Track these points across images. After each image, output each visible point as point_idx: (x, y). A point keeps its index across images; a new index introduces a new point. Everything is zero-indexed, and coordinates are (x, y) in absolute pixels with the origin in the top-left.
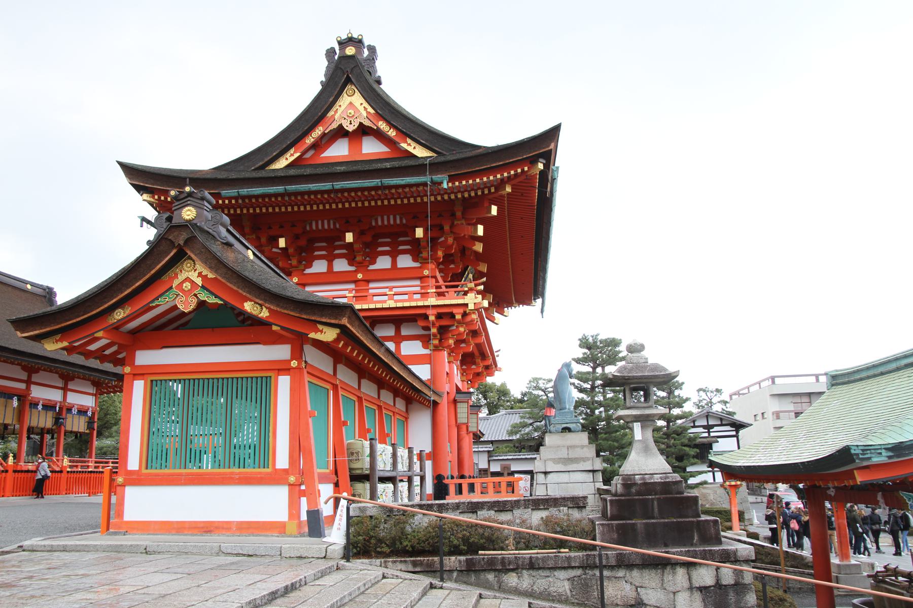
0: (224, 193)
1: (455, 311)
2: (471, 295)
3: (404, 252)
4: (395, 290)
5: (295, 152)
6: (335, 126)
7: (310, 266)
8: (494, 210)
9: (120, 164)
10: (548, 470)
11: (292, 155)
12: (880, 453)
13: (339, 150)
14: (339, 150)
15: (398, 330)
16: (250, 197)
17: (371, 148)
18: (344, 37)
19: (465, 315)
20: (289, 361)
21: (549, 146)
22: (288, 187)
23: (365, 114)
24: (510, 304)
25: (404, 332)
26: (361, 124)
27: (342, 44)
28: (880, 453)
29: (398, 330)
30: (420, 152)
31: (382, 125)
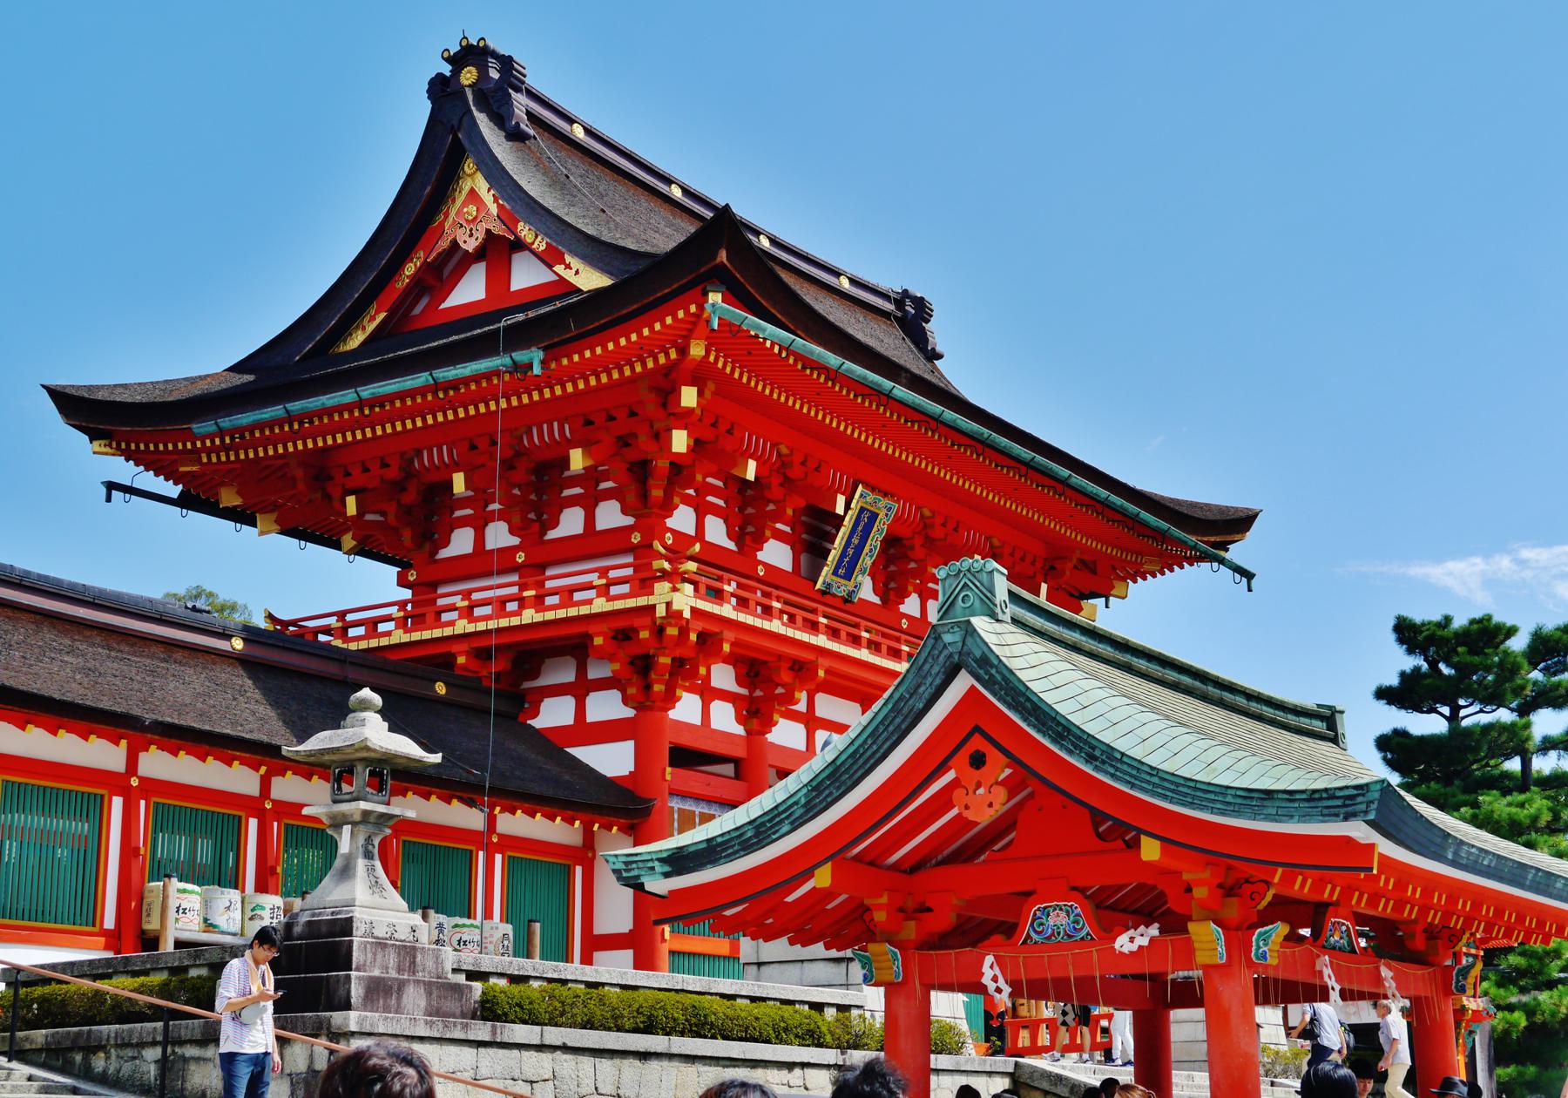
0: (199, 428)
1: (637, 622)
2: (662, 588)
3: (608, 495)
4: (475, 596)
5: (377, 312)
6: (444, 244)
7: (446, 543)
8: (689, 397)
10: (764, 959)
11: (373, 319)
12: (653, 868)
13: (471, 290)
14: (471, 290)
15: (581, 671)
16: (241, 430)
17: (526, 275)
22: (290, 406)
23: (494, 209)
24: (1138, 573)
25: (594, 673)
26: (488, 231)
27: (458, 60)
28: (653, 868)
29: (581, 671)
30: (589, 279)
31: (525, 231)
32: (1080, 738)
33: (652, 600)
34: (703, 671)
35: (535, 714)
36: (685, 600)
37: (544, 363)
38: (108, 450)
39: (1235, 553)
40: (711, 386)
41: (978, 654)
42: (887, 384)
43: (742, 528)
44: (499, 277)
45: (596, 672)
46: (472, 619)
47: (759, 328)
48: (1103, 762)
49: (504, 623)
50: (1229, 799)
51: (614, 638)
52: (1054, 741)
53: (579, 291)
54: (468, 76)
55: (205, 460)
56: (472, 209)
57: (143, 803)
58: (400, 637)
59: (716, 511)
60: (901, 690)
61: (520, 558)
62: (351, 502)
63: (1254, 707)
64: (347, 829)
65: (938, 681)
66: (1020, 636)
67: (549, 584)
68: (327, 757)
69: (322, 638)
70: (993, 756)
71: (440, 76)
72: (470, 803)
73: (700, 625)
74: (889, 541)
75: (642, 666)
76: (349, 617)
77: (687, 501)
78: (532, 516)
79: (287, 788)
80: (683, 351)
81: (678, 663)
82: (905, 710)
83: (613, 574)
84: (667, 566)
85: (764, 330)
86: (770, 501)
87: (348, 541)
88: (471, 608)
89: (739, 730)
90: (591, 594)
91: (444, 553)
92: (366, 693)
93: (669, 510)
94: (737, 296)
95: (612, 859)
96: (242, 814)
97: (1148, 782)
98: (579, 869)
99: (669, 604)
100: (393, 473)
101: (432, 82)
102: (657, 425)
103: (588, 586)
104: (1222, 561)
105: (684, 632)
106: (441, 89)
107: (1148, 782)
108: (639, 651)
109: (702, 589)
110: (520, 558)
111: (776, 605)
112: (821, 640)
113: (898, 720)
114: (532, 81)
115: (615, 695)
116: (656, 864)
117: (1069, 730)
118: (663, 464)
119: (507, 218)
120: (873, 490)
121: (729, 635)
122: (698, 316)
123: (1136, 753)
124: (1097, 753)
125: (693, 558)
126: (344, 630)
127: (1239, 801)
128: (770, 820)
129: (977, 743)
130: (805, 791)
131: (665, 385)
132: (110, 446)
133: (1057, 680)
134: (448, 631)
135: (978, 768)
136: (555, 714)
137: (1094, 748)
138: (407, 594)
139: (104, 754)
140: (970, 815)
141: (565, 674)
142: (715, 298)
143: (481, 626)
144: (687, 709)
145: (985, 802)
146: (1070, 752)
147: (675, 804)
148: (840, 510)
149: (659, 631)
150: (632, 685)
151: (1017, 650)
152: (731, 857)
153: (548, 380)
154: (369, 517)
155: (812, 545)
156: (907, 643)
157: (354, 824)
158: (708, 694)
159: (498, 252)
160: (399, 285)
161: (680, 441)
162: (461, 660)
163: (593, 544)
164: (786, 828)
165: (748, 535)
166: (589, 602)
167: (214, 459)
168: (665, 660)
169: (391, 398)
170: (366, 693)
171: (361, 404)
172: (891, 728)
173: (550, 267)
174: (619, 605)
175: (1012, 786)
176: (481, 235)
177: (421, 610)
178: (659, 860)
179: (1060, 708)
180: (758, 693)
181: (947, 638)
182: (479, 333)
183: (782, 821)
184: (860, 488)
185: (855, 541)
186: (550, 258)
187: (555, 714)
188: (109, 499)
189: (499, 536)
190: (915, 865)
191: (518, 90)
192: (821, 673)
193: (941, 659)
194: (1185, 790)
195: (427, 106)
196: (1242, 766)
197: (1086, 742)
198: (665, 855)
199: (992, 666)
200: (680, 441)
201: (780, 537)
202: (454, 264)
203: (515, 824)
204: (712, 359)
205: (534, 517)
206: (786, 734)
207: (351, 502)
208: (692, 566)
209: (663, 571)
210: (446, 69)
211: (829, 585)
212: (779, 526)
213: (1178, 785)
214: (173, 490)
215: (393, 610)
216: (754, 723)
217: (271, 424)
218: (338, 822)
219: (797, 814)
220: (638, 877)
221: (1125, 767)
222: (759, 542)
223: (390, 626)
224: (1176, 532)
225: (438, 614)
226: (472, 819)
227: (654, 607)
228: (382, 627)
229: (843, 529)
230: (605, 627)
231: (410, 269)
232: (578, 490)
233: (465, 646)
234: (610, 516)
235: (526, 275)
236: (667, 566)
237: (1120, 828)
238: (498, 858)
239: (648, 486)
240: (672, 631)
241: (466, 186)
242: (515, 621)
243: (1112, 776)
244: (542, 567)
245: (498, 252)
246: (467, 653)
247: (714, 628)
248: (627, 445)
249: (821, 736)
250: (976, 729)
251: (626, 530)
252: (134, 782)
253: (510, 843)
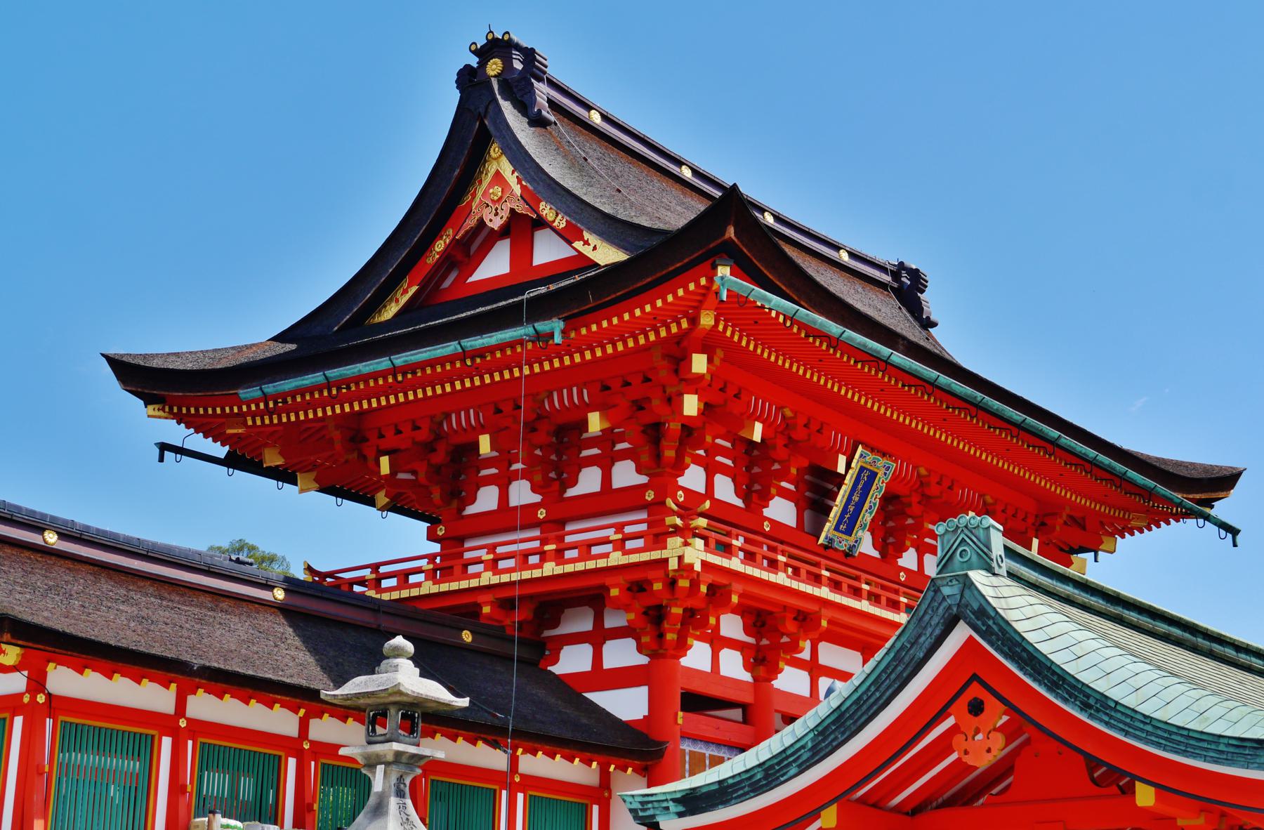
0: (244, 393)
1: (651, 575)
2: (674, 542)
3: (624, 455)
5: (410, 286)
6: (471, 223)
8: (699, 364)
9: (111, 361)
11: (405, 292)
12: (667, 808)
13: (496, 264)
14: (496, 264)
15: (599, 620)
16: (284, 396)
17: (547, 250)
18: (481, 42)
20: (21, 695)
21: (724, 234)
23: (517, 190)
24: (1126, 529)
26: (512, 210)
28: (667, 808)
29: (599, 620)
31: (546, 210)
32: (1074, 687)
33: (664, 554)
34: (712, 621)
35: (555, 660)
36: (696, 554)
37: (564, 332)
38: (161, 413)
39: (1220, 509)
40: (720, 353)
41: (976, 606)
42: (885, 351)
43: (749, 487)
44: (522, 253)
45: (613, 620)
46: (497, 571)
47: (765, 299)
48: (1098, 710)
49: (526, 575)
50: (1222, 748)
51: (629, 589)
52: (1050, 689)
53: (596, 265)
54: (494, 67)
55: (250, 423)
56: (497, 190)
57: (190, 743)
58: (429, 588)
59: (724, 470)
60: (903, 639)
61: (542, 514)
62: (385, 462)
63: (1243, 658)
64: (380, 769)
65: (937, 632)
66: (1016, 589)
67: (568, 539)
68: (362, 701)
69: (357, 589)
70: (991, 703)
71: (468, 67)
72: (494, 744)
73: (710, 578)
74: (888, 498)
75: (656, 616)
76: (383, 570)
77: (698, 461)
78: (553, 475)
79: (324, 729)
80: (694, 321)
81: (690, 613)
82: (907, 659)
83: (628, 529)
84: (679, 522)
85: (769, 301)
86: (775, 461)
87: (382, 498)
88: (495, 562)
89: (747, 677)
90: (609, 548)
91: (471, 510)
92: (399, 641)
93: (680, 469)
94: (745, 269)
95: (629, 799)
96: (283, 754)
97: (1142, 730)
98: (596, 808)
99: (680, 558)
100: (423, 435)
101: (460, 73)
102: (669, 390)
103: (605, 541)
104: (1207, 518)
105: (695, 584)
106: (469, 80)
107: (1142, 730)
108: (652, 602)
109: (712, 544)
110: (542, 514)
111: (782, 558)
112: (824, 592)
113: (900, 668)
114: (552, 71)
115: (630, 643)
116: (671, 804)
117: (1064, 680)
118: (675, 426)
119: (529, 198)
120: (872, 450)
121: (738, 587)
122: (708, 288)
123: (1130, 701)
124: (1092, 701)
125: (703, 515)
126: (378, 581)
127: (1231, 750)
128: (778, 764)
129: (975, 691)
130: (811, 735)
131: (677, 352)
132: (163, 410)
133: (1052, 631)
134: (474, 583)
135: (976, 715)
136: (574, 660)
137: (1088, 696)
138: (436, 548)
139: (154, 697)
140: (968, 760)
141: (584, 623)
142: (724, 271)
143: (505, 578)
144: (697, 657)
145: (984, 748)
146: (1065, 700)
147: (687, 746)
148: (841, 469)
149: (672, 583)
150: (645, 634)
151: (1013, 602)
152: (742, 798)
153: (568, 348)
154: (401, 476)
155: (815, 499)
156: (906, 595)
157: (387, 764)
158: (718, 643)
159: (521, 229)
160: (430, 261)
161: (691, 405)
162: (486, 610)
163: (610, 501)
164: (793, 771)
165: (755, 493)
166: (606, 555)
167: (259, 422)
168: (677, 610)
169: (422, 365)
170: (399, 641)
171: (394, 371)
172: (893, 676)
173: (570, 243)
174: (634, 558)
175: (1009, 732)
176: (505, 214)
177: (449, 562)
178: (674, 800)
179: (1057, 659)
180: (765, 642)
181: (946, 591)
182: (502, 306)
183: (789, 764)
184: (860, 448)
185: (856, 498)
186: (569, 235)
187: (574, 660)
188: (161, 459)
189: (522, 494)
190: (916, 808)
191: (540, 80)
192: (824, 623)
193: (941, 610)
194: (1179, 738)
195: (457, 95)
196: (1235, 715)
197: (1081, 691)
198: (678, 795)
199: (989, 617)
200: (691, 405)
201: (784, 494)
202: (481, 240)
203: (536, 764)
204: (721, 328)
205: (554, 475)
206: (791, 681)
207: (385, 462)
208: (702, 522)
209: (675, 526)
210: (474, 61)
211: (831, 540)
212: (784, 484)
213: (1170, 733)
214: (221, 451)
215: (423, 563)
216: (761, 671)
217: (311, 389)
218: (372, 764)
219: (804, 758)
220: (653, 816)
221: (1118, 715)
222: (765, 499)
223: (420, 578)
224: (1162, 490)
225: (465, 566)
226: (495, 759)
227: (666, 560)
228: (413, 579)
229: (844, 487)
230: (621, 579)
231: (440, 246)
232: (595, 451)
233: (490, 597)
234: (626, 475)
235: (547, 250)
236: (679, 522)
237: (1114, 774)
238: (520, 796)
239: (661, 447)
240: (683, 583)
241: (492, 168)
242: (537, 573)
243: (1107, 723)
244: (562, 523)
245: (521, 229)
246: (491, 603)
247: (722, 580)
248: (642, 408)
249: (824, 683)
250: (975, 677)
251: (641, 488)
252: (183, 723)
253: (531, 783)
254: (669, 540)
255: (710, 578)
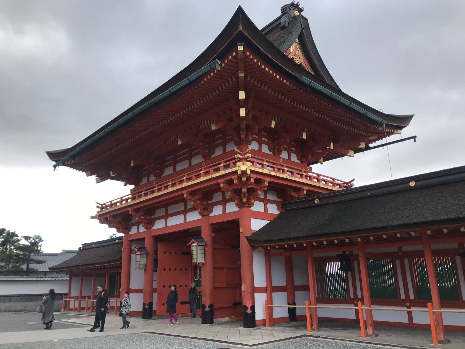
8: (242, 95)
19: (240, 179)
43: (274, 148)
80: (237, 77)
84: (240, 156)
93: (249, 143)
105: (249, 179)
121: (268, 179)
142: (241, 48)
158: (266, 201)
161: (243, 112)
168: (244, 190)
192: (305, 192)
200: (243, 112)
209: (239, 158)
227: (236, 172)
236: (240, 156)
240: (244, 179)
254: (237, 163)
255: (254, 176)
